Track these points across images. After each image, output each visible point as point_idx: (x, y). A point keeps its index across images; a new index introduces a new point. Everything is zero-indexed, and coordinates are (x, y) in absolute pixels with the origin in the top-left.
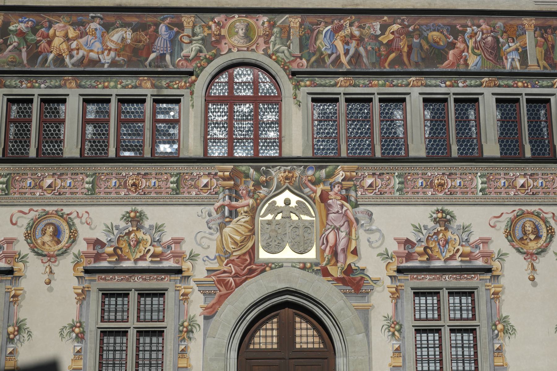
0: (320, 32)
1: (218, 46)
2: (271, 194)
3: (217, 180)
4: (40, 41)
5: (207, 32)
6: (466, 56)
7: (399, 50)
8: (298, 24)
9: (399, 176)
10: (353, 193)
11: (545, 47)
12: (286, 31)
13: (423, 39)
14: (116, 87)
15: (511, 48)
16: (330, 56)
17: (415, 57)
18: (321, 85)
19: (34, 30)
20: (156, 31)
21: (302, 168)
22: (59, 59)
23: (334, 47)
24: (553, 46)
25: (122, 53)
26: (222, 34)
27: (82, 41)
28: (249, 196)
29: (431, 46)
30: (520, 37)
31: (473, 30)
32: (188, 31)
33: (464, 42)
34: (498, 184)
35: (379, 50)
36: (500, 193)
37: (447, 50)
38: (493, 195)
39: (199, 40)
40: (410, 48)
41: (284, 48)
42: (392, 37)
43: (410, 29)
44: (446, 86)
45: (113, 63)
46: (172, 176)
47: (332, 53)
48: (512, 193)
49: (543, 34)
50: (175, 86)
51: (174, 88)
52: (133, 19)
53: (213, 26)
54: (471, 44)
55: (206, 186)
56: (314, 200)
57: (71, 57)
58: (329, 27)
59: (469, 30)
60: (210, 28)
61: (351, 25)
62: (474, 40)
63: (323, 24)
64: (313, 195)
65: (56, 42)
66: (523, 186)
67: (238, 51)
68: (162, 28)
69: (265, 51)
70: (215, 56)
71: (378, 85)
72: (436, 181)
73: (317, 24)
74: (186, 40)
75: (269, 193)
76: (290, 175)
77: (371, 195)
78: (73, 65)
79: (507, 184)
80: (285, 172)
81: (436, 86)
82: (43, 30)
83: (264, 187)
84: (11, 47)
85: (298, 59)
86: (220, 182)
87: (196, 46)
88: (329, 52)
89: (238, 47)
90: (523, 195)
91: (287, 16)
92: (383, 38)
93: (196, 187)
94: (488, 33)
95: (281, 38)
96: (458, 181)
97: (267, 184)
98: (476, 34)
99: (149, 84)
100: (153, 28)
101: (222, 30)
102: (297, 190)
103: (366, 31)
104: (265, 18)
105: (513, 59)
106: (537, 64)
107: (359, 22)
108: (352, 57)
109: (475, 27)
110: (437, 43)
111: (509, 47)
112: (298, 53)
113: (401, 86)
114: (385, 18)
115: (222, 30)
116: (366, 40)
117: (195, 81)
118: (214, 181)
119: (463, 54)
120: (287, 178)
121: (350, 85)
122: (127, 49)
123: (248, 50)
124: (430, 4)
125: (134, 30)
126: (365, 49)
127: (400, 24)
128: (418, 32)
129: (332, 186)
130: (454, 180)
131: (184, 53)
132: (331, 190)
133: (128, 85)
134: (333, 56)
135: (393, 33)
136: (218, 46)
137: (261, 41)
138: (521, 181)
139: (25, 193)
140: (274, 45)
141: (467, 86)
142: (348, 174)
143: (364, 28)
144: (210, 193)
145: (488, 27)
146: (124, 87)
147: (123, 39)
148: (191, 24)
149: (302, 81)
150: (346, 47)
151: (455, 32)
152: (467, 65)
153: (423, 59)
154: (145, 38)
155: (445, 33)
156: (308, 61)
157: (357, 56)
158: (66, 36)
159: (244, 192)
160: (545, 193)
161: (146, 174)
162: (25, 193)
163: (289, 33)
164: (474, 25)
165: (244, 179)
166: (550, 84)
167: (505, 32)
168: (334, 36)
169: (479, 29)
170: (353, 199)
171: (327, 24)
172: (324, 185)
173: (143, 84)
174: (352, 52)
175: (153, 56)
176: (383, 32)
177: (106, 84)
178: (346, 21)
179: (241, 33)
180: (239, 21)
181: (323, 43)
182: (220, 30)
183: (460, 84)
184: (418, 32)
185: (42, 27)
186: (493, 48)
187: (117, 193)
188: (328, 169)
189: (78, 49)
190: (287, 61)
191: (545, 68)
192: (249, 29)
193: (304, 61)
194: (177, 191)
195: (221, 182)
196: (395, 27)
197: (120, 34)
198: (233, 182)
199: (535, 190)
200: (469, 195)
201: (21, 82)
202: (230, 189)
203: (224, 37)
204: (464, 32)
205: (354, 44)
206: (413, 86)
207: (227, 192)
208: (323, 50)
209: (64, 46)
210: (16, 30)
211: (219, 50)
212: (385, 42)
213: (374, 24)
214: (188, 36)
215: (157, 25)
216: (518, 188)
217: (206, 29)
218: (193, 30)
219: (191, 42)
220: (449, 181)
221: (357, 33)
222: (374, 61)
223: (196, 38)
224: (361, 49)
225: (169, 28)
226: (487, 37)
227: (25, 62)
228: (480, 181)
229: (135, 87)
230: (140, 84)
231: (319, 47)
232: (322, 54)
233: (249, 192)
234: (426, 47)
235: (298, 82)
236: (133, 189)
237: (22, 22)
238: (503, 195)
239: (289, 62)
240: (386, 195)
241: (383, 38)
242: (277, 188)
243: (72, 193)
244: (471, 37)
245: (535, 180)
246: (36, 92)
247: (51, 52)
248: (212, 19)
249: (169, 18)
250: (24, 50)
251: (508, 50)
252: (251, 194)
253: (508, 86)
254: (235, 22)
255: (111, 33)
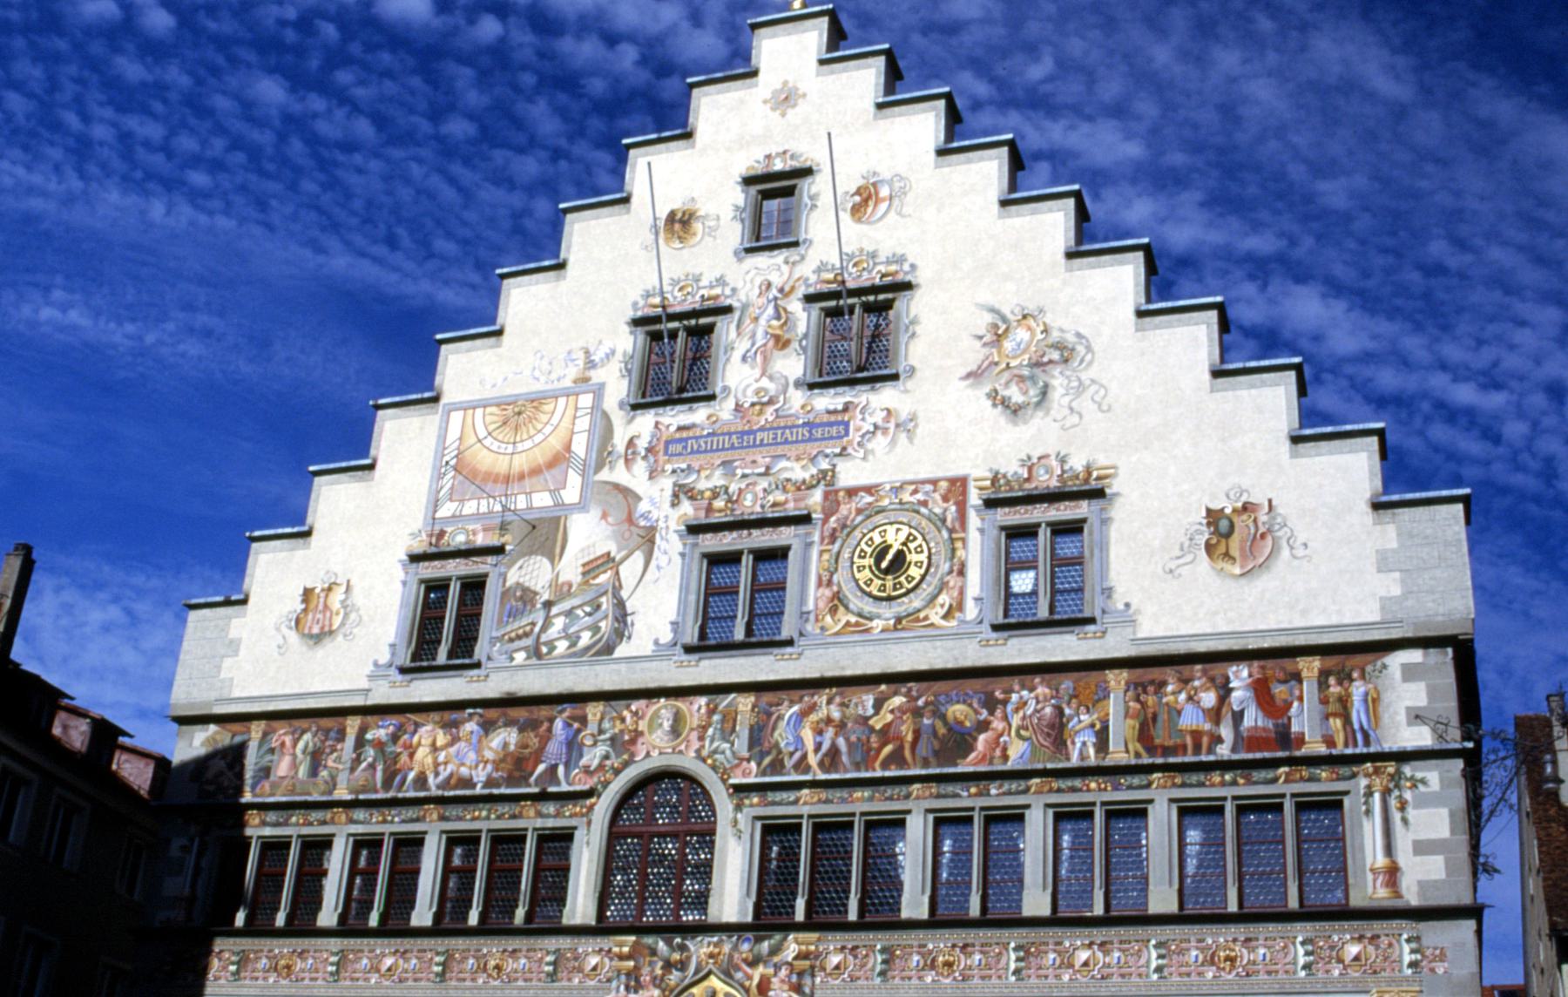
0: (780, 718)
1: (632, 748)
2: (687, 982)
3: (611, 959)
4: (400, 754)
5: (619, 726)
6: (1005, 742)
7: (900, 739)
8: (750, 707)
9: (883, 951)
10: (807, 981)
11: (1142, 718)
12: (730, 718)
13: (939, 717)
14: (488, 818)
15: (1082, 725)
16: (792, 754)
17: (923, 749)
18: (774, 803)
19: (395, 738)
20: (550, 730)
21: (735, 938)
22: (421, 781)
23: (799, 740)
24: (1155, 717)
25: (502, 765)
26: (640, 729)
27: (452, 750)
28: (656, 986)
29: (950, 729)
30: (1100, 705)
31: (1021, 697)
32: (592, 727)
33: (1005, 718)
34: (1044, 961)
35: (868, 741)
36: (1046, 977)
37: (975, 734)
38: (1033, 980)
39: (604, 741)
40: (917, 734)
41: (726, 746)
42: (889, 717)
43: (920, 702)
44: (970, 796)
45: (489, 783)
46: (548, 953)
47: (796, 750)
48: (1066, 978)
49: (1138, 695)
50: (567, 814)
51: (565, 817)
52: (521, 713)
53: (628, 720)
54: (1016, 721)
55: (594, 969)
56: (747, 990)
57: (437, 774)
58: (796, 708)
59: (1015, 697)
60: (623, 720)
61: (829, 702)
62: (1021, 714)
63: (786, 703)
64: (747, 983)
65: (422, 753)
66: (1086, 964)
67: (661, 753)
68: (559, 724)
69: (698, 751)
70: (626, 764)
71: (862, 799)
72: (941, 959)
73: (778, 704)
74: (588, 742)
75: (682, 981)
76: (717, 950)
77: (837, 982)
78: (438, 787)
79: (1058, 962)
80: (709, 944)
81: (956, 796)
82: (406, 737)
83: (677, 970)
84: (364, 765)
85: (745, 763)
86: (614, 963)
87: (601, 749)
88: (791, 749)
89: (660, 748)
90: (1085, 980)
91: (733, 696)
92: (877, 722)
93: (580, 970)
94: (1046, 700)
95: (722, 730)
96: (977, 957)
97: (682, 966)
98: (1025, 703)
99: (532, 813)
100: (546, 725)
101: (640, 722)
102: (727, 974)
103: (851, 711)
104: (702, 701)
105: (1084, 744)
106: (1123, 749)
107: (841, 694)
108: (826, 755)
109: (1025, 693)
110: (961, 723)
111: (1080, 721)
112: (746, 754)
113: (898, 799)
114: (883, 687)
115: (640, 722)
116: (850, 725)
117: (594, 804)
118: (606, 960)
119: (1002, 739)
120: (711, 956)
121: (820, 801)
122: (509, 759)
123: (673, 752)
124: (956, 659)
125: (521, 730)
126: (847, 740)
127: (905, 696)
128: (931, 707)
129: (777, 967)
130: (971, 954)
131: (583, 762)
132: (775, 974)
133: (503, 814)
134: (798, 755)
135: (892, 711)
136: (632, 748)
137: (694, 735)
138: (1083, 955)
139: (357, 980)
140: (712, 741)
141: (1004, 794)
142: (803, 948)
143: (847, 706)
144: (600, 981)
145: (1047, 691)
146: (499, 818)
147: (506, 745)
148: (599, 715)
149: (747, 797)
150: (818, 739)
151: (991, 704)
152: (1005, 758)
153: (936, 753)
154: (534, 741)
155: (976, 705)
156: (759, 765)
157: (834, 752)
158: (433, 744)
159: (648, 978)
160: (1123, 976)
161: (514, 951)
162: (357, 980)
163: (735, 721)
164: (1023, 687)
165: (648, 959)
166: (1145, 782)
167: (1076, 696)
168: (801, 721)
169: (1032, 695)
170: (807, 990)
171: (792, 703)
172: (765, 967)
173: (524, 813)
174: (826, 747)
175: (541, 768)
176: (877, 712)
177: (477, 813)
178: (821, 698)
179: (667, 725)
180: (665, 707)
181: (782, 736)
182: (637, 723)
183: (993, 791)
184: (931, 707)
185: (405, 732)
186: (1052, 726)
187: (473, 980)
188: (772, 941)
189: (446, 763)
190: (728, 766)
191: (1138, 755)
192: (678, 718)
193: (753, 765)
194: (552, 976)
195: (616, 963)
196: (898, 701)
197: (502, 736)
198: (632, 963)
199: (1106, 971)
200: (994, 980)
201: (371, 815)
202: (628, 975)
203: (642, 734)
204: (1005, 702)
205: (830, 733)
206: (918, 798)
207: (623, 978)
208: (782, 745)
209: (429, 760)
210: (373, 740)
211: (632, 755)
212: (878, 727)
213: (864, 698)
214: (593, 735)
215: (551, 720)
216: (1077, 967)
217: (618, 722)
218: (600, 724)
219: (595, 744)
220: (962, 956)
221: (836, 715)
222: (858, 758)
223: (602, 737)
224: (841, 742)
225: (568, 725)
226: (1043, 708)
227: (379, 785)
228: (1013, 956)
229: (513, 817)
230: (521, 813)
231: (777, 745)
232: (780, 752)
233: (654, 978)
234: (942, 731)
235: (741, 799)
236: (495, 974)
237: (382, 727)
238: (1051, 980)
239: (732, 768)
240: (859, 982)
241: (877, 722)
242: (696, 973)
243: (416, 980)
244: (1017, 710)
245: (1106, 953)
246: (387, 829)
247: (412, 769)
248: (628, 707)
249: (569, 710)
250: (380, 768)
251: (1077, 728)
252: (657, 982)
253: (1073, 790)
254: (659, 709)
255: (490, 737)
